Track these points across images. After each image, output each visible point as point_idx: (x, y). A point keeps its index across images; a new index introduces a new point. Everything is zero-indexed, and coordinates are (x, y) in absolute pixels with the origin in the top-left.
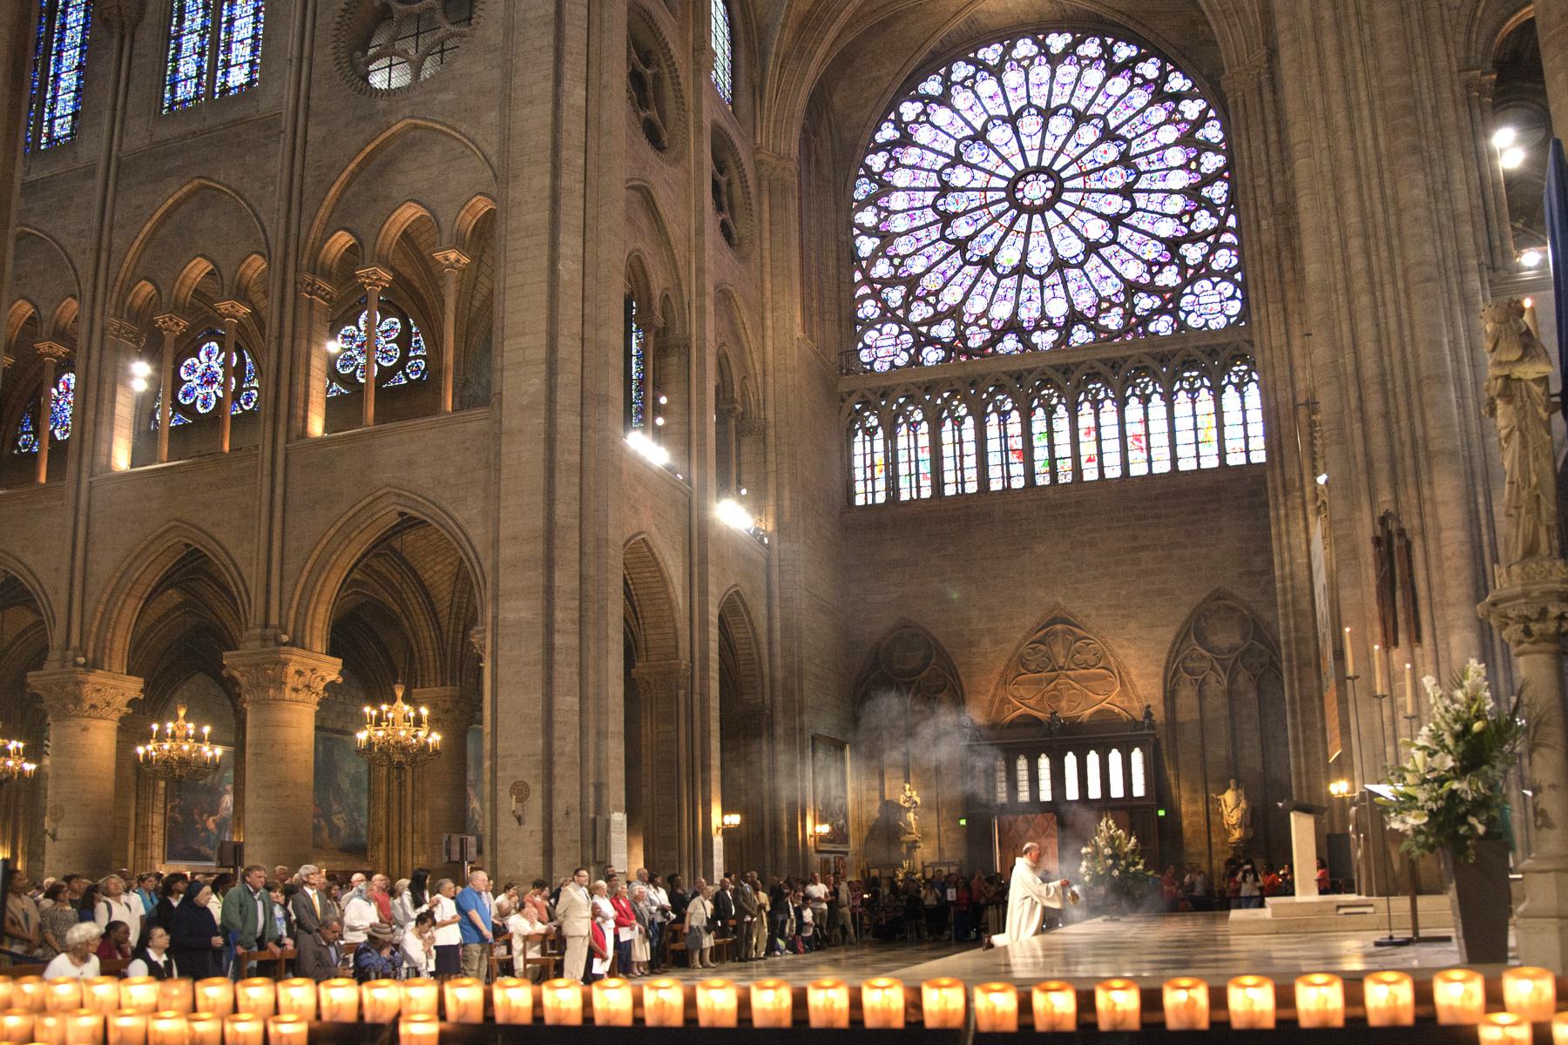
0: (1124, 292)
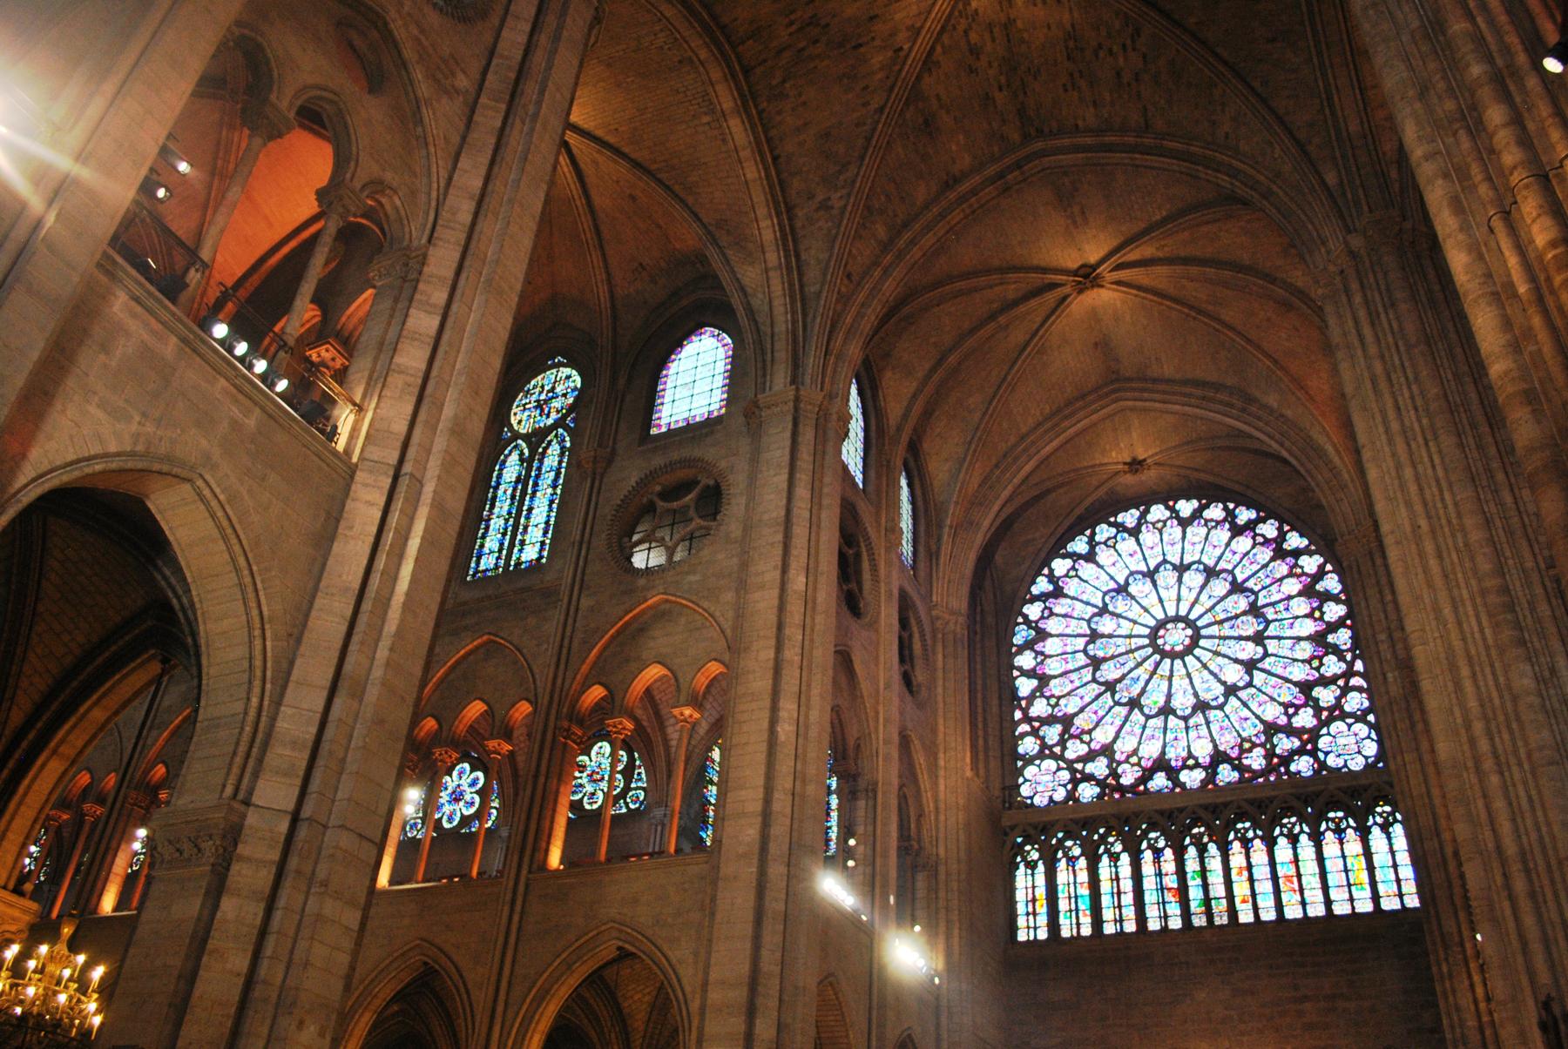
0: (1264, 732)
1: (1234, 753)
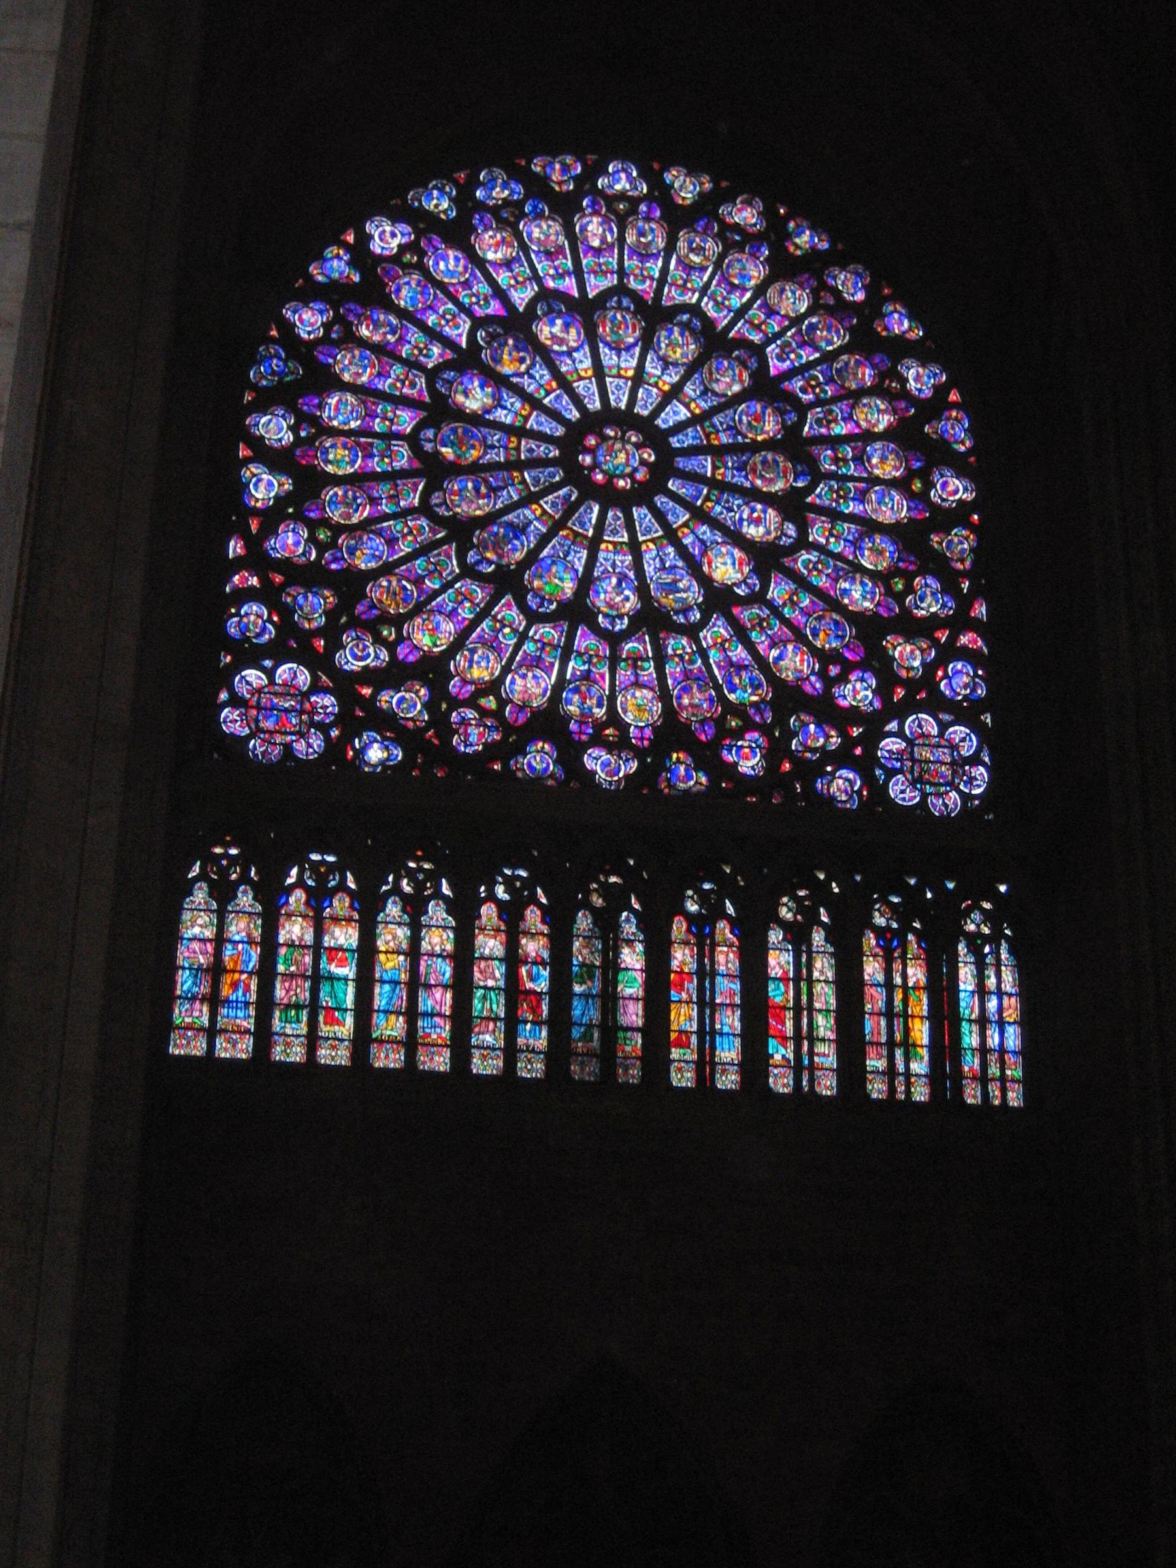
0: (774, 705)
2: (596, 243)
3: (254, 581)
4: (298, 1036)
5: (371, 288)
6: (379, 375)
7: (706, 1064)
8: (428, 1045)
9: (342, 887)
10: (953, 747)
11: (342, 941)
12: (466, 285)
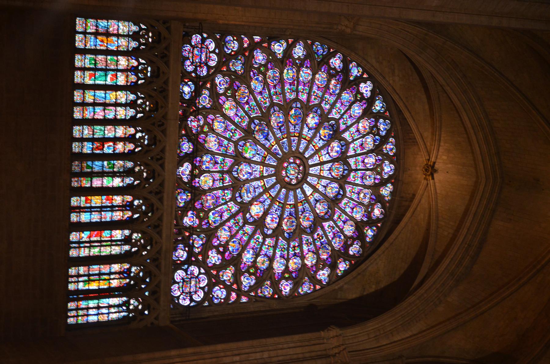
1: (198, 205)
2: (366, 161)
3: (246, 45)
4: (85, 64)
5: (349, 84)
6: (319, 87)
7: (79, 209)
8: (83, 110)
9: (139, 78)
10: (196, 292)
11: (119, 79)
12: (350, 117)
